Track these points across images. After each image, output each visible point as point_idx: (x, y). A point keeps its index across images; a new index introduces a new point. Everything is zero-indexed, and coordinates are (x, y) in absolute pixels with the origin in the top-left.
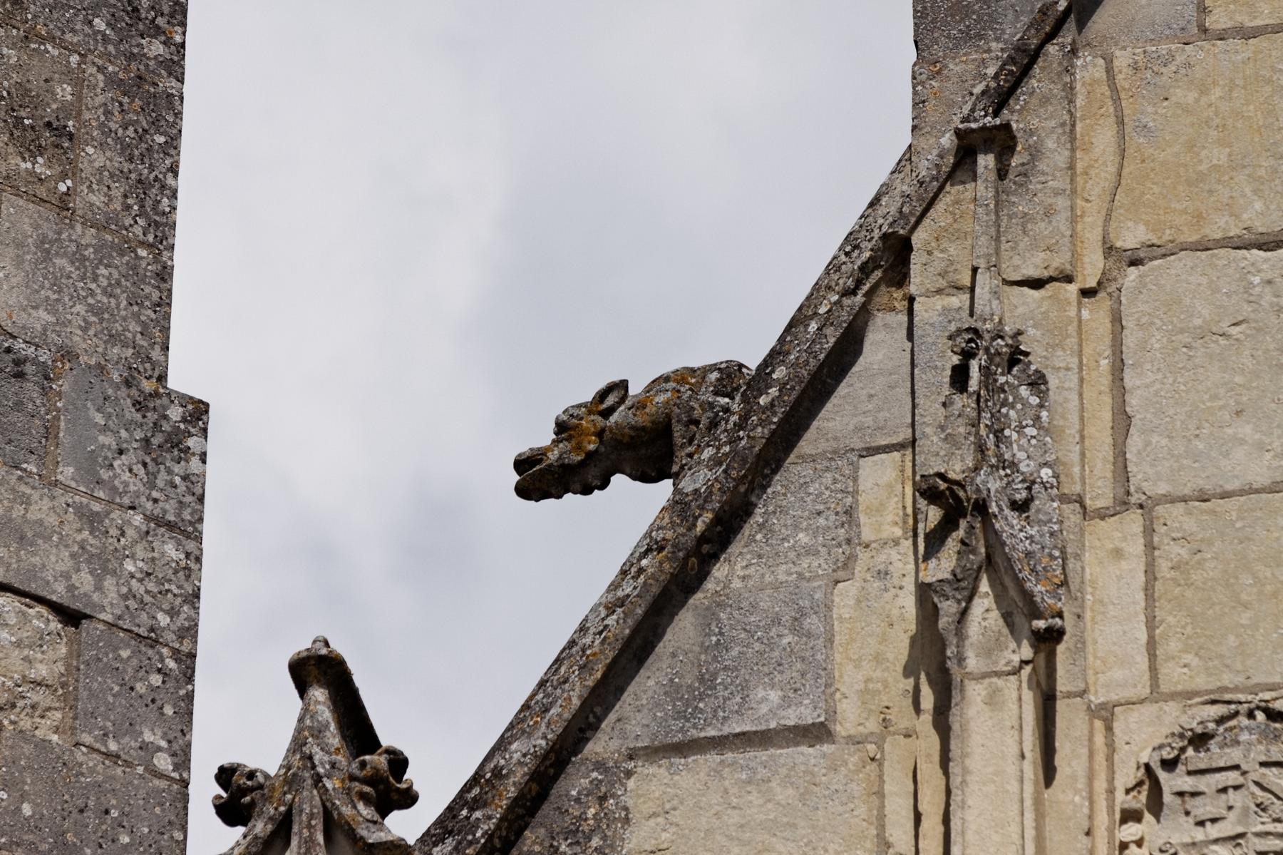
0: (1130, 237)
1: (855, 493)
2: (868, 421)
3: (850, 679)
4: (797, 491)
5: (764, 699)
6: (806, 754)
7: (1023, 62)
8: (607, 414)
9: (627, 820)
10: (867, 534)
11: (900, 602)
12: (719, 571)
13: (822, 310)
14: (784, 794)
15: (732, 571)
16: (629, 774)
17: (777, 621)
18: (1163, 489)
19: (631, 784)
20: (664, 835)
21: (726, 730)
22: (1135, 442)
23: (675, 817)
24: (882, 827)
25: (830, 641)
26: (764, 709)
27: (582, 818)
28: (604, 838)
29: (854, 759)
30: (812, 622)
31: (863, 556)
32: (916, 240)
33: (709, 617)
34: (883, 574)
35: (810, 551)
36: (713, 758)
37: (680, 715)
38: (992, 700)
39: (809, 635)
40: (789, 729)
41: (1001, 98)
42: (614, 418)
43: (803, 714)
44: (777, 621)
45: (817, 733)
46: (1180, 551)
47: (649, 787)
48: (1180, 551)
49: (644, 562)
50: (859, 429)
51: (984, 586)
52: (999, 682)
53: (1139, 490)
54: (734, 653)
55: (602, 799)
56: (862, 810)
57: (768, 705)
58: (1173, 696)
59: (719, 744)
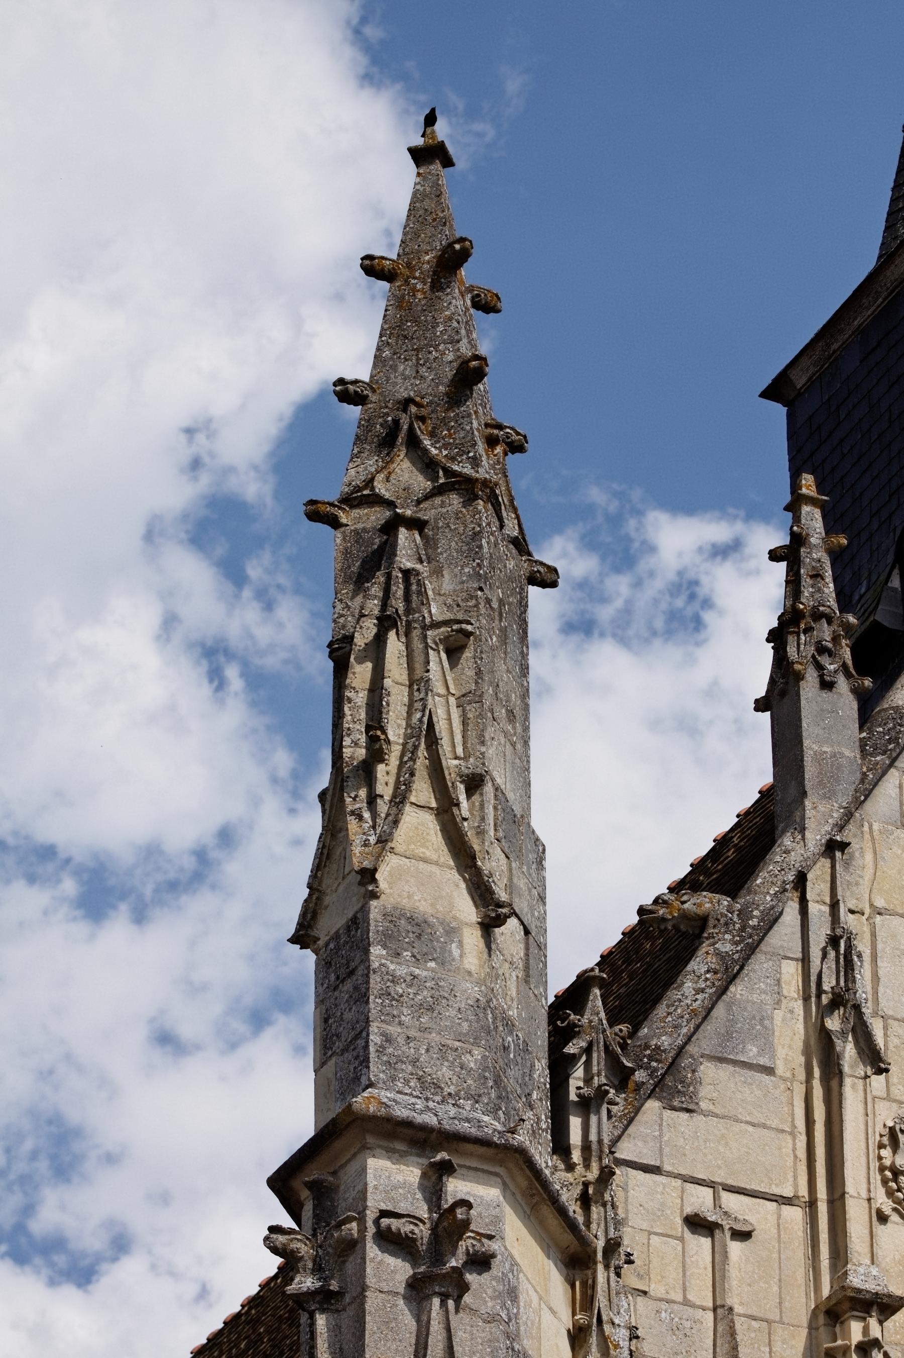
0: (880, 903)
1: (780, 973)
2: (785, 945)
3: (781, 1052)
4: (759, 965)
5: (751, 1050)
6: (765, 1078)
7: (848, 816)
8: (683, 903)
9: (701, 1083)
10: (785, 992)
11: (798, 1026)
12: (732, 989)
13: (772, 892)
14: (758, 1093)
15: (736, 989)
16: (701, 1064)
17: (754, 1018)
18: (890, 1013)
19: (702, 1067)
20: (714, 1094)
21: (737, 1059)
22: (881, 990)
23: (719, 1087)
24: (793, 1119)
25: (773, 1033)
26: (751, 1054)
27: (686, 1076)
28: (695, 1088)
29: (782, 1086)
30: (766, 1022)
31: (784, 1001)
32: (810, 876)
33: (729, 1006)
34: (791, 1012)
35: (765, 992)
36: (730, 1068)
37: (720, 1045)
38: (854, 1086)
39: (766, 1028)
40: (760, 1065)
41: (841, 828)
42: (686, 906)
43: (763, 1061)
44: (754, 1018)
45: (769, 1071)
46: (896, 1041)
47: (708, 1071)
48: (896, 1041)
49: (708, 976)
50: (782, 947)
51: (850, 1038)
52: (856, 1080)
53: (882, 1010)
54: (739, 1025)
55: (694, 1071)
56: (786, 1109)
57: (751, 1053)
58: (895, 1101)
59: (735, 1063)
